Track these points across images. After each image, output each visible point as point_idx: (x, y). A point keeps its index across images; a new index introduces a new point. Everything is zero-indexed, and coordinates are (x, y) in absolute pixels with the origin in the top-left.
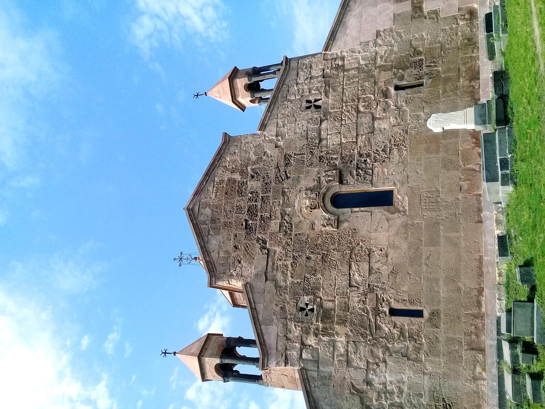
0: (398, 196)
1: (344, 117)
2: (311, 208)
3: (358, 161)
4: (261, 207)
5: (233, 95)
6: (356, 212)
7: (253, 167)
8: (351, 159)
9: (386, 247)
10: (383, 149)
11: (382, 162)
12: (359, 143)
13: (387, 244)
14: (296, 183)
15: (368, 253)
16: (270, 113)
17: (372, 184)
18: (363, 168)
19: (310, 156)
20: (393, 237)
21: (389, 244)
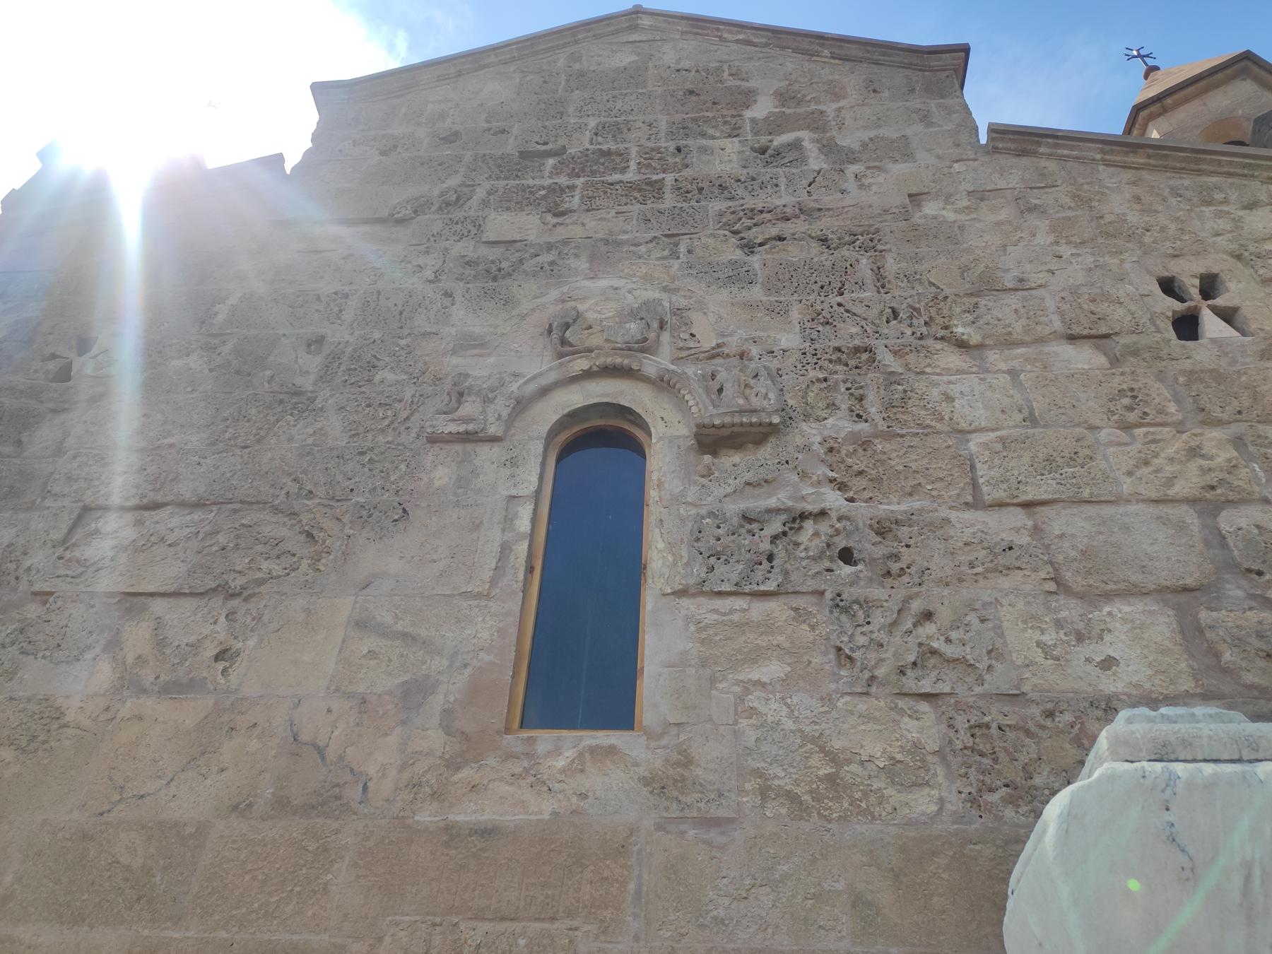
1: (1146, 434)
3: (840, 519)
4: (612, 184)
5: (1169, 101)
6: (508, 521)
7: (806, 144)
8: (858, 483)
10: (934, 652)
11: (839, 649)
12: (967, 523)
15: (237, 583)
16: (1098, 156)
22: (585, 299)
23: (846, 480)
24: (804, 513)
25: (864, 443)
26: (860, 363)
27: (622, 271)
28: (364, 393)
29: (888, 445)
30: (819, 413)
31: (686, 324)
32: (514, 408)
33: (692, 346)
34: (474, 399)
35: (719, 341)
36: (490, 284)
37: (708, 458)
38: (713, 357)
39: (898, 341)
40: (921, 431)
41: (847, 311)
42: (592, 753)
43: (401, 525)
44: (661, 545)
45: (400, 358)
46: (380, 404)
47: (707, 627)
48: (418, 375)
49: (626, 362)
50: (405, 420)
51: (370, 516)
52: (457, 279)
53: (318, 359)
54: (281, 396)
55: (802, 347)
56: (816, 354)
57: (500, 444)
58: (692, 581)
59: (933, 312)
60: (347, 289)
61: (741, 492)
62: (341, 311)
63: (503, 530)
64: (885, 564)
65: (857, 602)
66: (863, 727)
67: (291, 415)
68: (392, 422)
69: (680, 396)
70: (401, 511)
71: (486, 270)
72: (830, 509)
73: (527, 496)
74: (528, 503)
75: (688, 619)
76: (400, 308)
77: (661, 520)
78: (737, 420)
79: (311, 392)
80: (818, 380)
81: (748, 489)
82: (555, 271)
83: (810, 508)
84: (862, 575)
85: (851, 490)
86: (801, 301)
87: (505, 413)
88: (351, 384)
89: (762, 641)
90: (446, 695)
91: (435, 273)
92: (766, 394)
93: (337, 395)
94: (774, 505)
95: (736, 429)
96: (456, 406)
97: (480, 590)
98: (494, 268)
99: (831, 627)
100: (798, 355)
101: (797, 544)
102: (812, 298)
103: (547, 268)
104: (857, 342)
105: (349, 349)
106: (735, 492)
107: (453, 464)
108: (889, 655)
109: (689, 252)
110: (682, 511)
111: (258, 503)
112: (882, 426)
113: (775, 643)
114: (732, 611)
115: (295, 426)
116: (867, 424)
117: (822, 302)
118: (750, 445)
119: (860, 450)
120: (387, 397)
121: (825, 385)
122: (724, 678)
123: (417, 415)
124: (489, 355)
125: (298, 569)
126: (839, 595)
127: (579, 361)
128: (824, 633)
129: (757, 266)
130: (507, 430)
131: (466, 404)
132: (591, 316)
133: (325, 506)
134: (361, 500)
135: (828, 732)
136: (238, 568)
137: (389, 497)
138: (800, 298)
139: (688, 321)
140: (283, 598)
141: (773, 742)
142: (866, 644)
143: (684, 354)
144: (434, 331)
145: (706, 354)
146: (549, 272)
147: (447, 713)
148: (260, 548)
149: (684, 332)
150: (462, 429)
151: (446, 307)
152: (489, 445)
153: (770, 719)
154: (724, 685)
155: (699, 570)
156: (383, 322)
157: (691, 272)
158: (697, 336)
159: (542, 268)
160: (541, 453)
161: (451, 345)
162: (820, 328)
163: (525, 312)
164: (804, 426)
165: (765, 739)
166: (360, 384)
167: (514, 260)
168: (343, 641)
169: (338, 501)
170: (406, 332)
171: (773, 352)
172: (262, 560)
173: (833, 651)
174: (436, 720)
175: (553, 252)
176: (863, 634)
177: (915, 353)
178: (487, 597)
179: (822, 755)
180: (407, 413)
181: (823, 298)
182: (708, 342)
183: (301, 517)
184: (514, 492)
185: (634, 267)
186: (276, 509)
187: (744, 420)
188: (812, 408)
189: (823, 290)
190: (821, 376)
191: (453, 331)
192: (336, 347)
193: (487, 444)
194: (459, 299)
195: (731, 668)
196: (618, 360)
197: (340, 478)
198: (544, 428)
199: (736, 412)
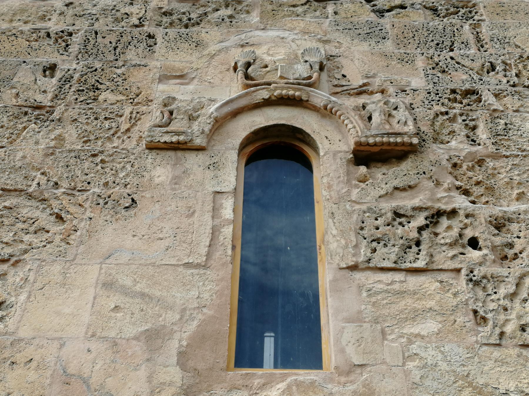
0: (282, 386)
2: (248, 65)
3: (467, 216)
6: (215, 211)
8: (477, 191)
9: (11, 328)
11: (475, 312)
13: (23, 333)
14: (360, 31)
17: (354, 268)
18: (436, 234)
19: (477, 65)
20: (51, 360)
21: (20, 340)
22: (259, 45)
23: (468, 187)
24: (439, 211)
25: (479, 161)
26: (470, 102)
27: (285, 25)
28: (91, 109)
29: (497, 163)
30: (444, 138)
31: (338, 68)
32: (213, 125)
33: (344, 84)
34: (182, 117)
35: (365, 81)
36: (183, 30)
37: (363, 169)
38: (360, 93)
39: (498, 87)
40: (520, 153)
41: (458, 63)
42: (297, 386)
43: (132, 212)
44: (335, 232)
45: (118, 83)
46: (106, 118)
47: (377, 293)
48: (134, 96)
49: (297, 94)
50: (126, 130)
51: (106, 203)
52: (157, 25)
53: (54, 81)
54: (26, 109)
55: (428, 88)
56: (438, 94)
57: (204, 152)
58: (361, 259)
59: (520, 66)
60: (71, 29)
61: (392, 194)
62: (67, 46)
63: (213, 217)
64: (503, 250)
65: (484, 277)
66: (499, 369)
67: (35, 123)
68: (116, 132)
69: (340, 121)
70: (131, 200)
71: (179, 19)
72: (460, 209)
73: (228, 192)
74: (230, 197)
75: (360, 288)
76: (114, 44)
77: (332, 213)
78: (385, 139)
79: (50, 107)
80: (442, 113)
81: (397, 193)
82: (233, 23)
83: (443, 207)
84: (487, 258)
85: (472, 195)
86: (423, 54)
87: (207, 129)
88: (81, 102)
89: (418, 305)
90: (180, 341)
91: (140, 19)
92: (406, 122)
93: (70, 110)
94: (417, 205)
95: (384, 147)
96: (168, 121)
97: (199, 261)
98: (185, 19)
99: (468, 295)
100: (424, 94)
101: (436, 234)
102: (431, 51)
103: (227, 20)
104: (467, 86)
105: (77, 76)
106: (387, 194)
107: (169, 167)
108: (513, 316)
109: (336, 13)
110: (348, 207)
111: (15, 190)
112: (492, 149)
113: (428, 306)
114: (393, 283)
115: (39, 132)
116: (480, 147)
117: (439, 56)
118: (394, 160)
119: (476, 166)
120: (111, 113)
121: (446, 117)
122: (392, 332)
123: (136, 128)
124: (187, 84)
125: (52, 242)
126: (472, 272)
127: (261, 91)
128: (464, 300)
129: (388, 27)
130: (209, 142)
131: (177, 120)
132: (267, 59)
133: (68, 194)
134: (97, 190)
135: (473, 372)
136: (5, 240)
137: (120, 189)
138: (421, 52)
139: (340, 66)
140: (44, 263)
141: (434, 379)
142: (495, 308)
143: (339, 89)
144: (143, 63)
145: (356, 91)
146: (228, 23)
147: (182, 355)
148: (20, 225)
149: (337, 73)
150: (175, 139)
151: (150, 46)
152: (196, 152)
153: (429, 363)
154: (393, 336)
155: (364, 252)
156: (101, 55)
157: (338, 28)
158: (348, 77)
159: (223, 20)
160: (236, 160)
161: (158, 75)
162: (439, 75)
163: (214, 53)
164: (434, 146)
165: (427, 377)
166: (88, 101)
167: (201, 13)
168: (95, 298)
169: (79, 191)
170: (120, 63)
171: (406, 91)
172: (23, 234)
173: (471, 314)
174: (174, 360)
175: (230, 8)
176: (493, 301)
177: (510, 96)
178: (205, 266)
179: (471, 389)
180: (128, 126)
181: (439, 53)
182: (357, 81)
183: (51, 202)
184: (218, 189)
185: (294, 22)
186: (30, 196)
187: (392, 140)
188: (438, 134)
189: (439, 47)
190: (443, 110)
191: (158, 64)
192: (66, 72)
193: (194, 152)
194: (159, 40)
195: (396, 324)
196: (291, 93)
197: (79, 173)
198: (237, 142)
199: (385, 134)
